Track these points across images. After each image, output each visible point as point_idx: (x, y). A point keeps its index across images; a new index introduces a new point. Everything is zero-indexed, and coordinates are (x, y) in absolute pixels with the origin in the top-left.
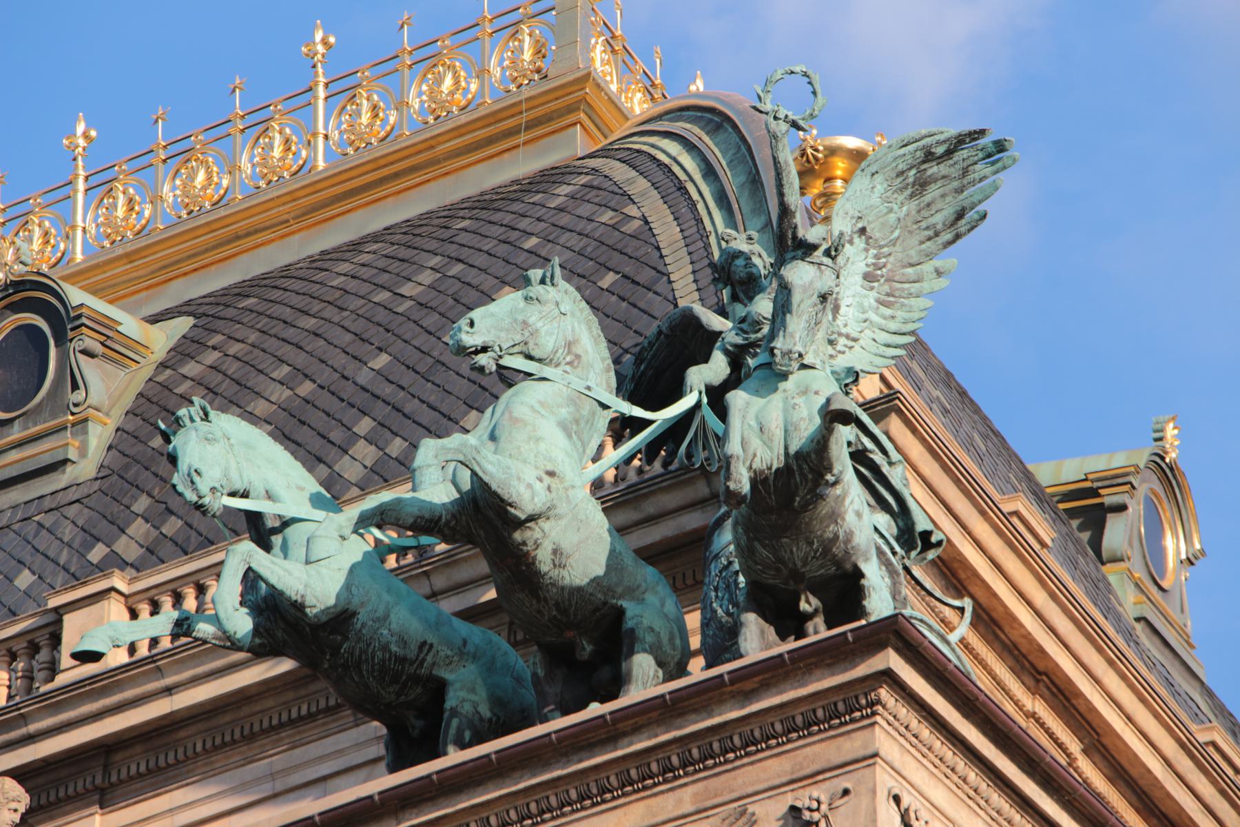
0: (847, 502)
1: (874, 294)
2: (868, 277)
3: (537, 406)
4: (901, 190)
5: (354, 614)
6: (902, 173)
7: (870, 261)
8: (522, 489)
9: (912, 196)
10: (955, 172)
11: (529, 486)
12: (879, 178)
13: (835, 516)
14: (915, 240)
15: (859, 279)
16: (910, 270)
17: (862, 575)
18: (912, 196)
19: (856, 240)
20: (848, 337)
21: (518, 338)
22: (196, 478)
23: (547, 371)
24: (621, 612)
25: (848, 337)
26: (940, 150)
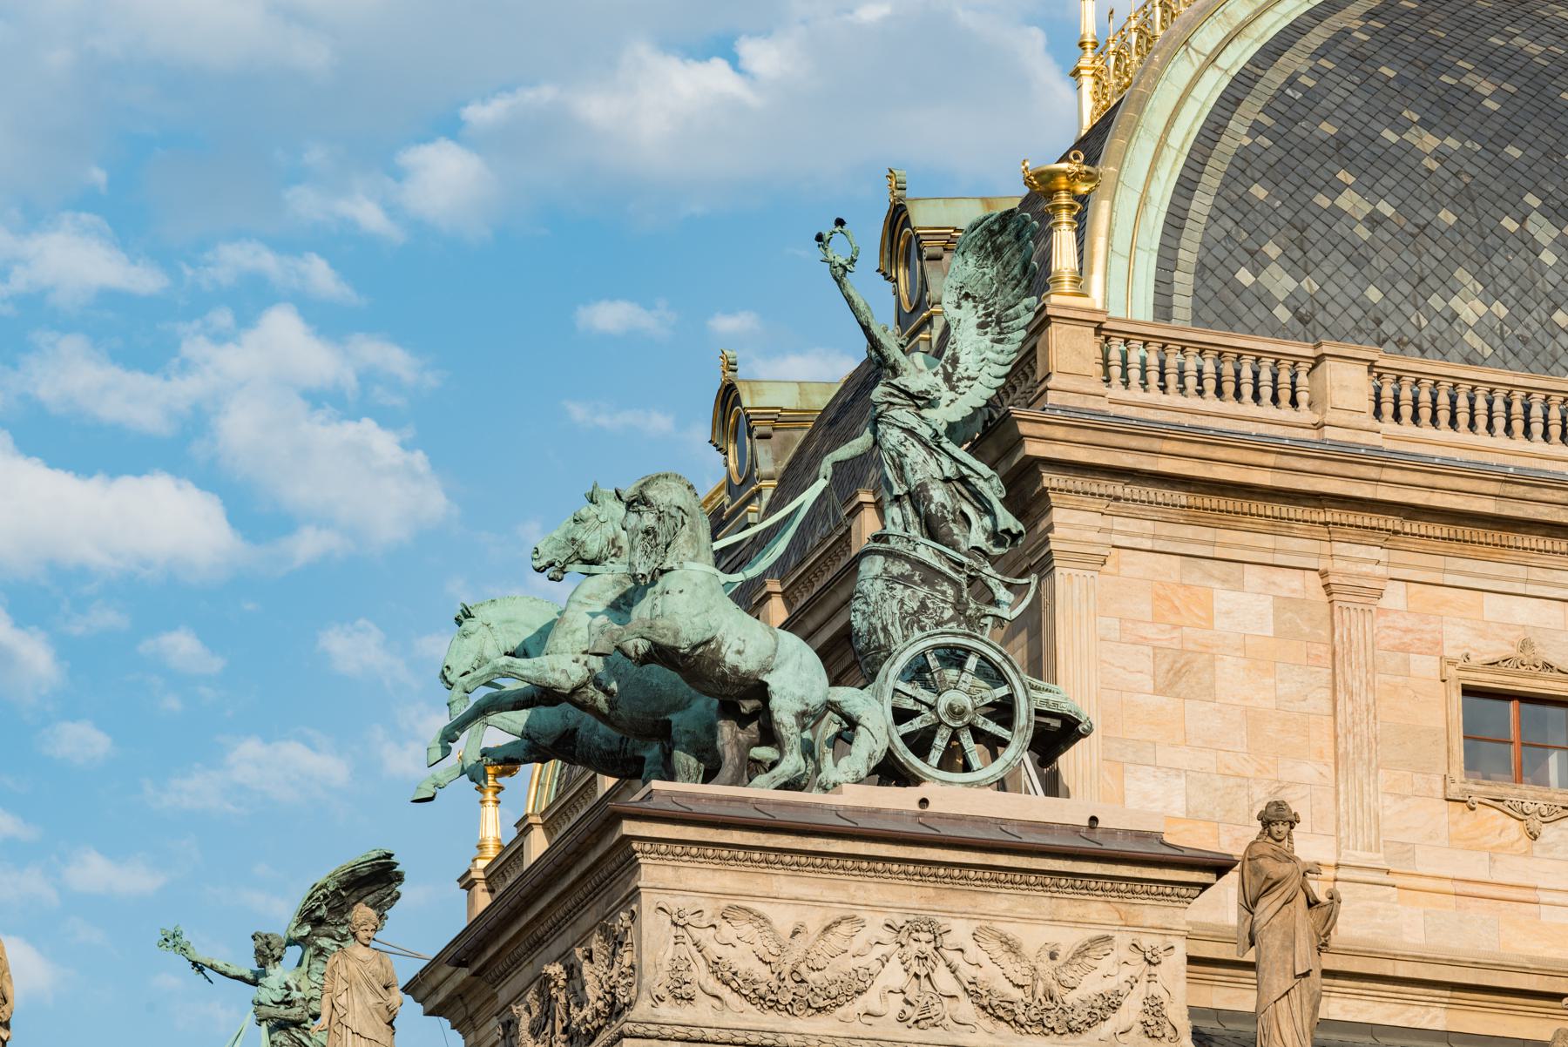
0: (723, 650)
1: (989, 336)
2: (982, 326)
3: (584, 600)
4: (987, 257)
5: (575, 730)
6: (981, 247)
7: (981, 312)
8: (557, 676)
9: (996, 259)
10: (1012, 238)
11: (564, 671)
12: (968, 254)
13: (717, 661)
14: (1008, 290)
15: (974, 331)
16: (1011, 311)
17: (766, 685)
18: (996, 259)
19: (963, 303)
20: (969, 378)
21: (570, 552)
22: (447, 674)
23: (594, 569)
24: (669, 722)
25: (969, 378)
26: (996, 227)
